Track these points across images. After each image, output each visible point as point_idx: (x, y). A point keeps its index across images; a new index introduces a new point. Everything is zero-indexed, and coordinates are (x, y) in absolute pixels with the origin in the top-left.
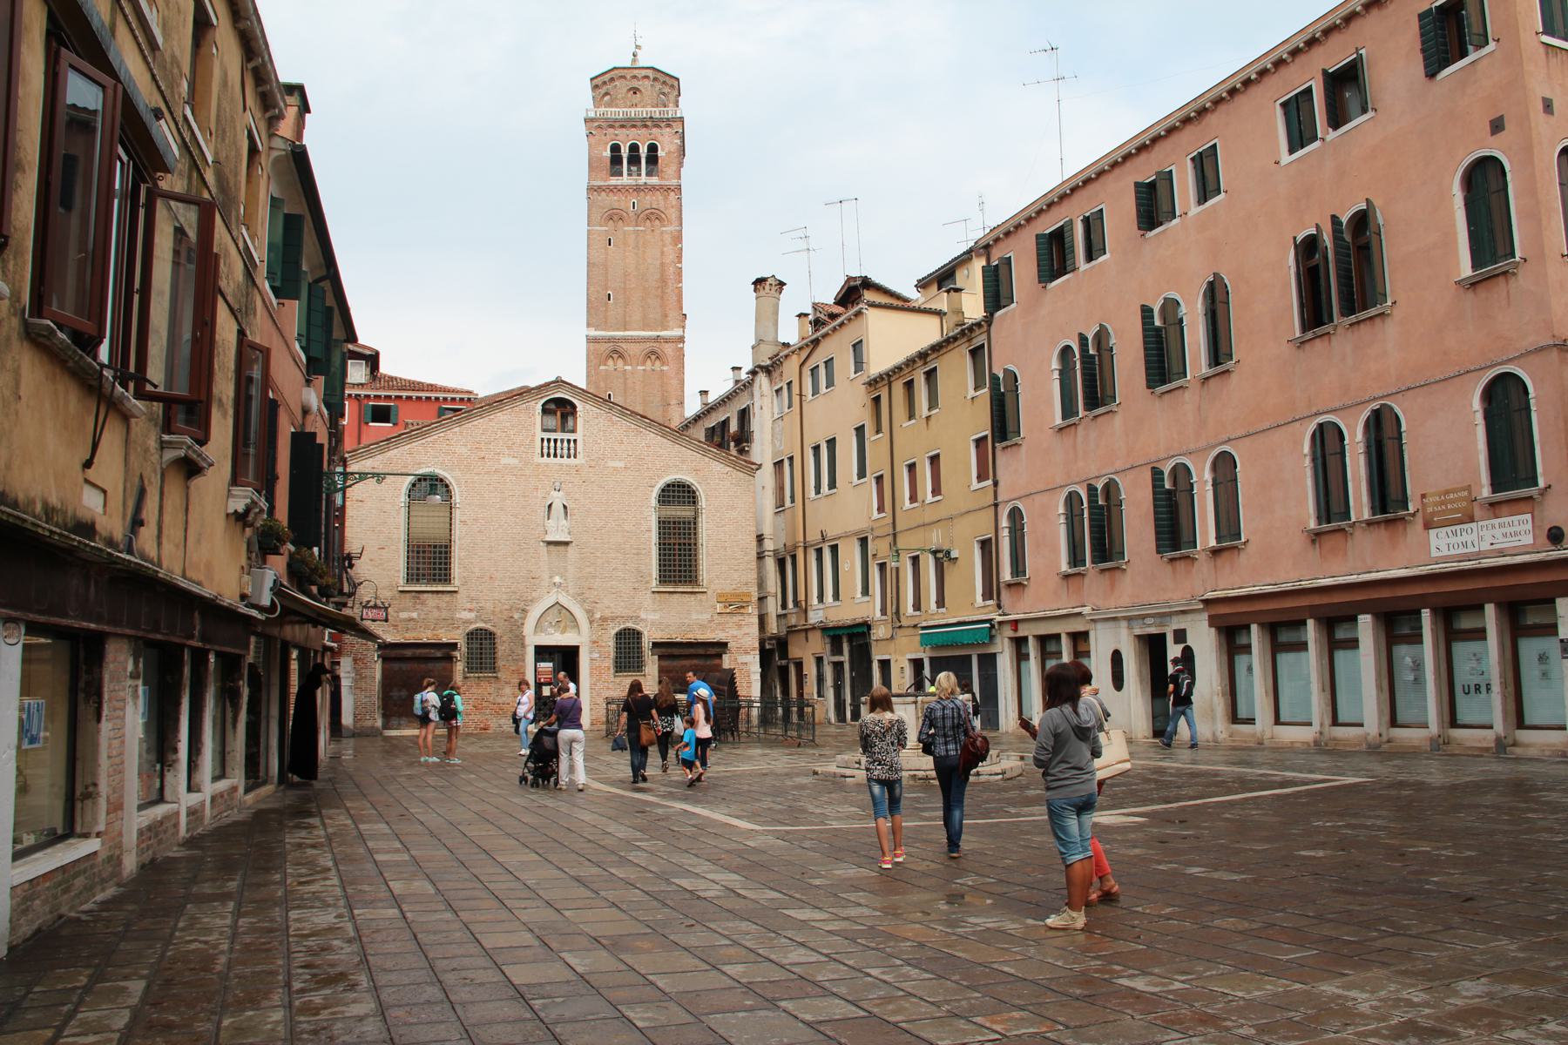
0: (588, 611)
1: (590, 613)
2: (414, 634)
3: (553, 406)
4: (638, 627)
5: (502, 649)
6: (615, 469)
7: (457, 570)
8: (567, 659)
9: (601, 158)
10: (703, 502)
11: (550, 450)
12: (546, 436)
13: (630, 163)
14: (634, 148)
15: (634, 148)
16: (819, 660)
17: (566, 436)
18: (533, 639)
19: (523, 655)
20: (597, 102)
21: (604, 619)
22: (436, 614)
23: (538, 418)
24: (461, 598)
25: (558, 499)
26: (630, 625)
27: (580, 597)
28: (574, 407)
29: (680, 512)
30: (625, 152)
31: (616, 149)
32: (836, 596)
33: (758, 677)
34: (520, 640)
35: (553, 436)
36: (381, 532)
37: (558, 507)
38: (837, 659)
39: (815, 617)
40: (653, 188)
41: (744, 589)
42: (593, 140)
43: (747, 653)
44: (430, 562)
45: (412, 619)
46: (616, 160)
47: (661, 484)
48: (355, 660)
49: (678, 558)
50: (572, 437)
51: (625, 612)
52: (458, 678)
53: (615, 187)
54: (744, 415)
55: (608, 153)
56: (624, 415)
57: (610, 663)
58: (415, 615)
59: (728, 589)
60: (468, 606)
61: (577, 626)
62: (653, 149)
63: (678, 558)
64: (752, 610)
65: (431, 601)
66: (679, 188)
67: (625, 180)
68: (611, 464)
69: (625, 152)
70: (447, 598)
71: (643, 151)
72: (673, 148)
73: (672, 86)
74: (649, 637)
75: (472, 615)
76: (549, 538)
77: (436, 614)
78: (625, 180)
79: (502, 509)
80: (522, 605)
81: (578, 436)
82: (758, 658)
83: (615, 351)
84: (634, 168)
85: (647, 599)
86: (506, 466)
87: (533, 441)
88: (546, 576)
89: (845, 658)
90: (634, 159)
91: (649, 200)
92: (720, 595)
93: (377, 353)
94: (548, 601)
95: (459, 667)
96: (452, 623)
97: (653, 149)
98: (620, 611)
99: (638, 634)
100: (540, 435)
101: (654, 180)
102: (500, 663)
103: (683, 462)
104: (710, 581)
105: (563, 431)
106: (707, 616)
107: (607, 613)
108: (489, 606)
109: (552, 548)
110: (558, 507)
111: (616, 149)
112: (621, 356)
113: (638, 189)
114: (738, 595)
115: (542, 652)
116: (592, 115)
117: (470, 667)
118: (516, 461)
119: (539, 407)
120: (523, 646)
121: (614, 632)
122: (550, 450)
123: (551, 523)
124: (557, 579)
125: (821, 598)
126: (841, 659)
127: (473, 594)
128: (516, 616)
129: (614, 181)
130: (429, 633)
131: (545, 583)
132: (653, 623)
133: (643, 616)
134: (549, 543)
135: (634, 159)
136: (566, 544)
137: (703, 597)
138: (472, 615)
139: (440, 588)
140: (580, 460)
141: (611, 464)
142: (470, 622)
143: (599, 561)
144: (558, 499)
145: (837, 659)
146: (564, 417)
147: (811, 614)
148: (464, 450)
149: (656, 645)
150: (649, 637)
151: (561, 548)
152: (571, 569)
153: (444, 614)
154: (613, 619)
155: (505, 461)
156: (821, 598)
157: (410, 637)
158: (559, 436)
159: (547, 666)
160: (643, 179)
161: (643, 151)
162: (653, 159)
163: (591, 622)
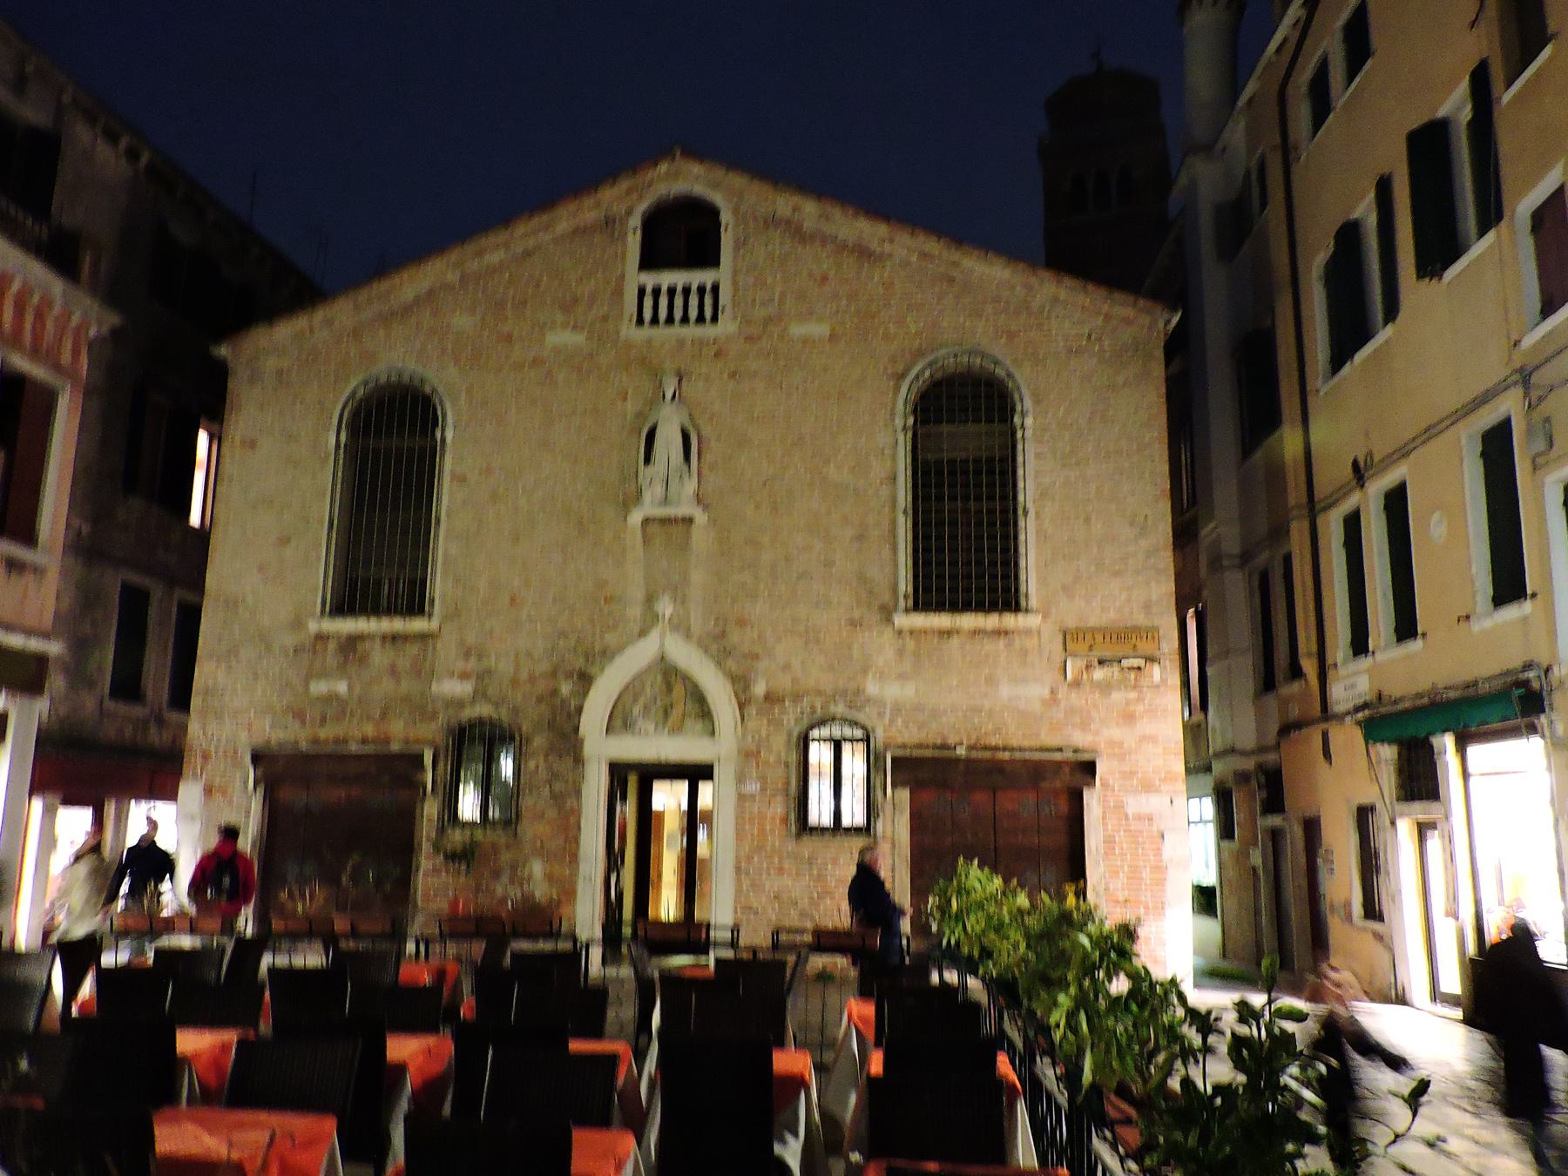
1: (741, 684)
6: (805, 341)
7: (440, 587)
12: (649, 280)
24: (447, 651)
29: (963, 440)
32: (1406, 627)
35: (667, 278)
45: (331, 698)
48: (208, 791)
51: (826, 681)
58: (342, 687)
68: (797, 330)
70: (413, 649)
77: (387, 685)
80: (580, 663)
86: (557, 350)
87: (619, 292)
88: (637, 593)
96: (421, 709)
107: (784, 683)
108: (505, 667)
109: (654, 529)
118: (579, 339)
120: (579, 760)
125: (1360, 645)
127: (471, 639)
128: (566, 688)
130: (369, 730)
132: (897, 709)
133: (872, 688)
140: (727, 326)
141: (797, 330)
142: (459, 704)
151: (676, 531)
152: (698, 577)
154: (797, 698)
156: (1360, 645)
163: (741, 706)
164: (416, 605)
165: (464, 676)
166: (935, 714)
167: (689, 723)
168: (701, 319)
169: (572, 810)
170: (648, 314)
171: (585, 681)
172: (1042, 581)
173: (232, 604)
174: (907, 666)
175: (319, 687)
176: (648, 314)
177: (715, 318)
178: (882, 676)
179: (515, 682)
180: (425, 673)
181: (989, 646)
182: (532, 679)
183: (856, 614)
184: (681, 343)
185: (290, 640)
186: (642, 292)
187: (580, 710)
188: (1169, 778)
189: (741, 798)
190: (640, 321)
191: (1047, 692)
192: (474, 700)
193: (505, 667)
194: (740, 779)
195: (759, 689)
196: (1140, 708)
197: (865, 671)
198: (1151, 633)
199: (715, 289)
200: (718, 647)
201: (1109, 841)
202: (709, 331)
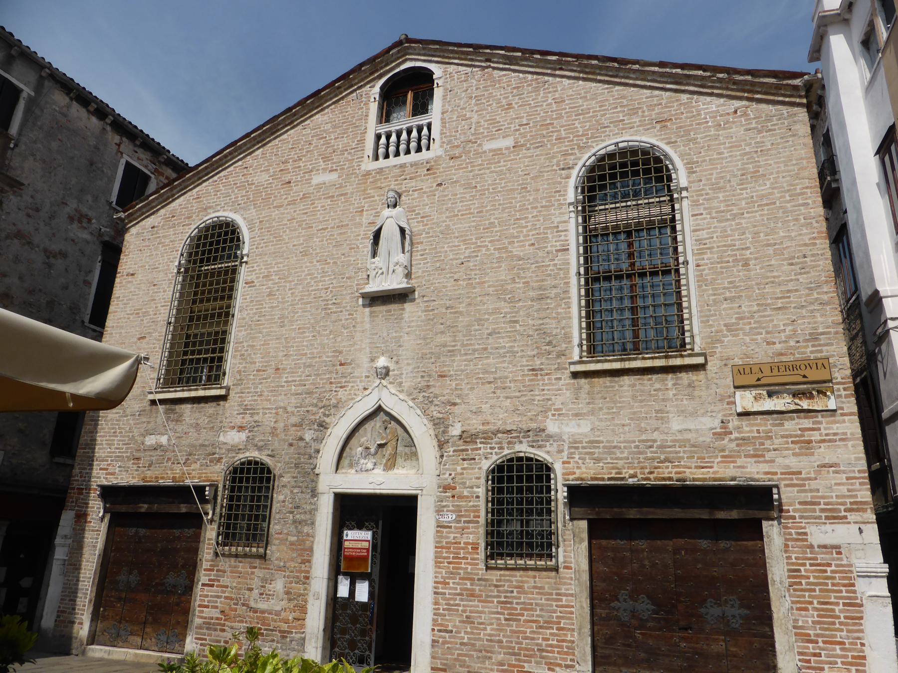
1: (440, 425)
4: (541, 455)
5: (281, 497)
6: (497, 152)
7: (231, 362)
8: (391, 519)
10: (681, 178)
12: (383, 129)
18: (334, 481)
19: (313, 512)
21: (468, 438)
22: (193, 437)
23: (374, 108)
26: (524, 449)
33: (881, 588)
34: (309, 479)
36: (146, 313)
37: (390, 234)
41: (809, 351)
43: (834, 517)
44: (198, 351)
45: (157, 447)
47: (586, 158)
52: (206, 554)
56: (511, 61)
57: (477, 535)
58: (164, 440)
59: (762, 354)
60: (239, 420)
61: (413, 455)
63: (632, 298)
64: (842, 401)
68: (488, 146)
70: (210, 408)
74: (563, 475)
76: (373, 287)
79: (305, 254)
82: (872, 534)
85: (562, 390)
86: (319, 186)
87: (362, 141)
92: (740, 370)
95: (210, 533)
98: (503, 418)
99: (543, 471)
100: (372, 126)
102: (275, 528)
103: (634, 112)
104: (714, 340)
106: (709, 423)
107: (475, 425)
108: (268, 420)
114: (793, 367)
115: (351, 509)
117: (228, 536)
118: (334, 176)
119: (375, 90)
120: (314, 493)
121: (486, 465)
122: (385, 147)
124: (382, 362)
128: (308, 436)
130: (178, 469)
132: (575, 444)
133: (552, 427)
140: (436, 149)
141: (488, 146)
142: (237, 449)
143: (463, 321)
144: (391, 220)
148: (265, 176)
149: (580, 495)
150: (563, 475)
153: (205, 436)
154: (487, 436)
155: (317, 179)
159: (359, 538)
163: (441, 445)
164: (215, 377)
165: (241, 428)
166: (611, 449)
167: (400, 461)
168: (419, 149)
169: (308, 535)
170: (381, 151)
171: (323, 426)
172: (705, 322)
174: (582, 407)
175: (150, 440)
176: (381, 151)
177: (428, 149)
178: (559, 414)
179: (274, 432)
181: (654, 382)
182: (286, 429)
183: (537, 362)
184: (402, 166)
186: (378, 137)
187: (318, 451)
188: (856, 507)
189: (440, 526)
190: (376, 158)
191: (717, 423)
192: (246, 449)
193: (268, 420)
194: (439, 511)
195: (456, 431)
196: (815, 436)
198: (824, 363)
199: (429, 126)
200: (424, 397)
201: (794, 573)
202: (425, 155)
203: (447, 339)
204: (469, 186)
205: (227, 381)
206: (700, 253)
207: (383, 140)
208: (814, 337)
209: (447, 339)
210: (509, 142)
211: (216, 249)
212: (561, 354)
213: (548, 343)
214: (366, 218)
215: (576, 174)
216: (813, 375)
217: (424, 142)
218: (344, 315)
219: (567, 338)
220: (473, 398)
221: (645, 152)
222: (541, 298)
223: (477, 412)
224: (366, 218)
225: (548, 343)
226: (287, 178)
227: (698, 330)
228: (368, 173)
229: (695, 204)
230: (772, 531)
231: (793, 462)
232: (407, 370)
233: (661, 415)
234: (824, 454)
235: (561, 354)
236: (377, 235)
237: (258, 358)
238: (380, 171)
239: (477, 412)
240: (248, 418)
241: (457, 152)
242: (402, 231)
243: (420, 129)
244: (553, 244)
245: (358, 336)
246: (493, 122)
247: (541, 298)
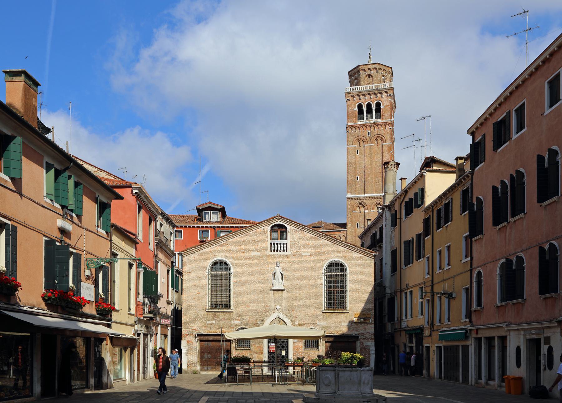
0: (292, 321)
1: (293, 322)
2: (214, 330)
3: (276, 228)
6: (305, 256)
9: (353, 112)
11: (275, 248)
12: (273, 242)
13: (367, 113)
14: (369, 105)
15: (369, 105)
16: (405, 345)
17: (282, 242)
20: (352, 84)
22: (223, 322)
23: (269, 234)
24: (234, 315)
25: (278, 270)
27: (289, 315)
28: (286, 228)
30: (365, 108)
31: (360, 106)
33: (374, 352)
35: (276, 242)
37: (278, 275)
38: (410, 345)
39: (404, 325)
40: (378, 125)
41: (368, 311)
42: (348, 102)
43: (368, 341)
46: (360, 112)
47: (327, 263)
48: (188, 341)
49: (336, 297)
50: (285, 242)
51: (310, 322)
53: (360, 125)
54: (381, 229)
55: (356, 109)
58: (214, 322)
60: (238, 318)
62: (378, 104)
63: (336, 297)
65: (221, 316)
66: (392, 123)
67: (365, 121)
68: (303, 254)
69: (365, 108)
70: (228, 315)
71: (374, 106)
72: (388, 103)
73: (388, 72)
75: (239, 322)
77: (223, 322)
78: (365, 121)
81: (288, 241)
82: (374, 344)
83: (361, 204)
84: (369, 115)
87: (266, 244)
88: (273, 305)
89: (414, 345)
90: (369, 111)
91: (376, 130)
93: (224, 208)
94: (274, 316)
97: (378, 104)
100: (270, 241)
101: (379, 120)
103: (339, 252)
104: (351, 308)
105: (282, 239)
107: (301, 322)
108: (247, 318)
110: (278, 275)
111: (360, 106)
112: (363, 206)
113: (371, 125)
116: (348, 91)
118: (259, 254)
119: (269, 229)
123: (274, 281)
125: (406, 316)
126: (413, 345)
127: (240, 313)
129: (359, 122)
131: (273, 308)
133: (318, 323)
134: (274, 290)
135: (369, 111)
136: (283, 290)
137: (347, 315)
138: (239, 322)
139: (225, 310)
141: (303, 254)
143: (298, 298)
144: (278, 270)
145: (410, 345)
146: (282, 233)
147: (402, 324)
151: (280, 292)
152: (284, 302)
153: (227, 322)
157: (212, 332)
158: (279, 242)
160: (374, 120)
161: (374, 106)
162: (378, 110)
165: (239, 320)
166: (330, 328)
170: (273, 249)
171: (263, 321)
173: (189, 306)
175: (209, 322)
176: (273, 249)
177: (287, 251)
179: (249, 321)
180: (230, 319)
181: (339, 315)
184: (280, 255)
185: (202, 313)
186: (271, 244)
188: (372, 339)
190: (271, 251)
192: (241, 325)
193: (247, 318)
195: (297, 323)
197: (317, 320)
198: (370, 314)
199: (286, 244)
203: (294, 302)
204: (298, 264)
205: (232, 308)
206: (350, 289)
207: (273, 245)
208: (369, 309)
209: (294, 302)
210: (308, 254)
211: (220, 268)
212: (320, 308)
213: (317, 305)
214: (270, 268)
215: (325, 266)
216: (368, 316)
217: (285, 249)
218: (266, 294)
219: (322, 305)
220: (300, 316)
221: (341, 264)
222: (316, 295)
223: (302, 319)
224: (270, 268)
225: (317, 305)
226: (243, 251)
227: (348, 305)
228: (269, 255)
229: (350, 278)
230: (358, 343)
231: (362, 331)
232: (284, 309)
233: (340, 322)
234: (368, 330)
235: (320, 308)
236: (275, 273)
237: (241, 303)
238: (273, 255)
239: (302, 319)
240: (240, 318)
241: (295, 254)
242: (282, 274)
243: (284, 244)
244: (319, 283)
245: (271, 300)
246: (304, 247)
247: (316, 295)
